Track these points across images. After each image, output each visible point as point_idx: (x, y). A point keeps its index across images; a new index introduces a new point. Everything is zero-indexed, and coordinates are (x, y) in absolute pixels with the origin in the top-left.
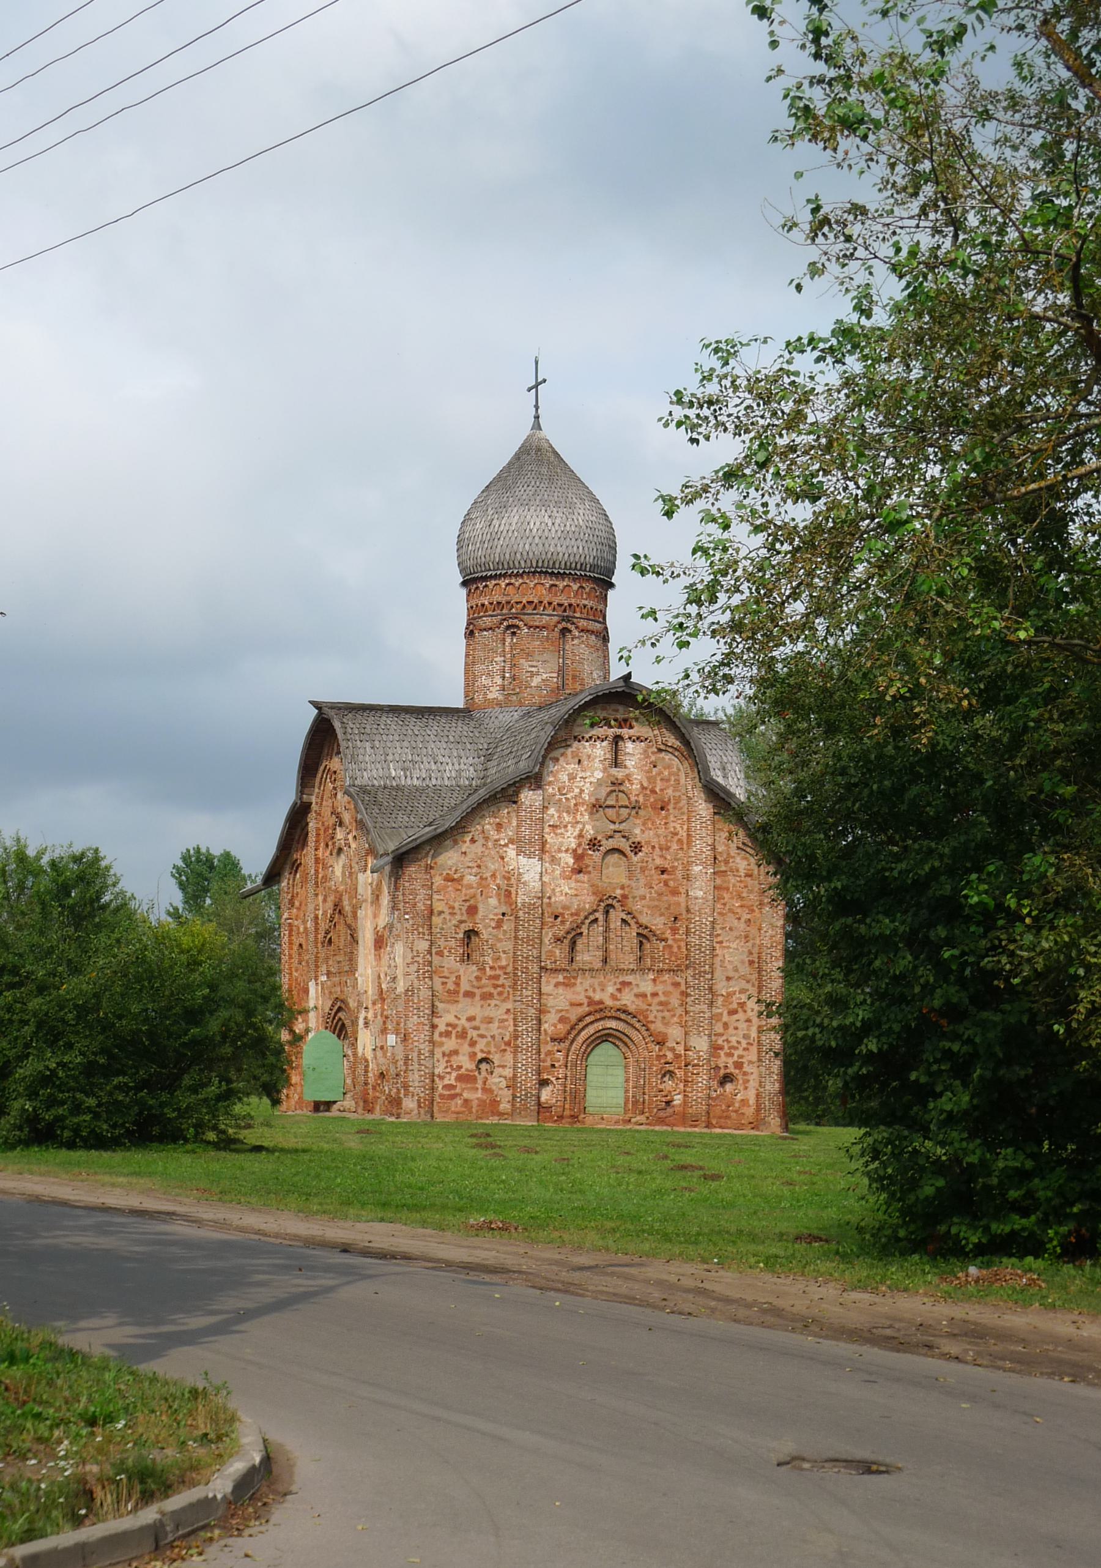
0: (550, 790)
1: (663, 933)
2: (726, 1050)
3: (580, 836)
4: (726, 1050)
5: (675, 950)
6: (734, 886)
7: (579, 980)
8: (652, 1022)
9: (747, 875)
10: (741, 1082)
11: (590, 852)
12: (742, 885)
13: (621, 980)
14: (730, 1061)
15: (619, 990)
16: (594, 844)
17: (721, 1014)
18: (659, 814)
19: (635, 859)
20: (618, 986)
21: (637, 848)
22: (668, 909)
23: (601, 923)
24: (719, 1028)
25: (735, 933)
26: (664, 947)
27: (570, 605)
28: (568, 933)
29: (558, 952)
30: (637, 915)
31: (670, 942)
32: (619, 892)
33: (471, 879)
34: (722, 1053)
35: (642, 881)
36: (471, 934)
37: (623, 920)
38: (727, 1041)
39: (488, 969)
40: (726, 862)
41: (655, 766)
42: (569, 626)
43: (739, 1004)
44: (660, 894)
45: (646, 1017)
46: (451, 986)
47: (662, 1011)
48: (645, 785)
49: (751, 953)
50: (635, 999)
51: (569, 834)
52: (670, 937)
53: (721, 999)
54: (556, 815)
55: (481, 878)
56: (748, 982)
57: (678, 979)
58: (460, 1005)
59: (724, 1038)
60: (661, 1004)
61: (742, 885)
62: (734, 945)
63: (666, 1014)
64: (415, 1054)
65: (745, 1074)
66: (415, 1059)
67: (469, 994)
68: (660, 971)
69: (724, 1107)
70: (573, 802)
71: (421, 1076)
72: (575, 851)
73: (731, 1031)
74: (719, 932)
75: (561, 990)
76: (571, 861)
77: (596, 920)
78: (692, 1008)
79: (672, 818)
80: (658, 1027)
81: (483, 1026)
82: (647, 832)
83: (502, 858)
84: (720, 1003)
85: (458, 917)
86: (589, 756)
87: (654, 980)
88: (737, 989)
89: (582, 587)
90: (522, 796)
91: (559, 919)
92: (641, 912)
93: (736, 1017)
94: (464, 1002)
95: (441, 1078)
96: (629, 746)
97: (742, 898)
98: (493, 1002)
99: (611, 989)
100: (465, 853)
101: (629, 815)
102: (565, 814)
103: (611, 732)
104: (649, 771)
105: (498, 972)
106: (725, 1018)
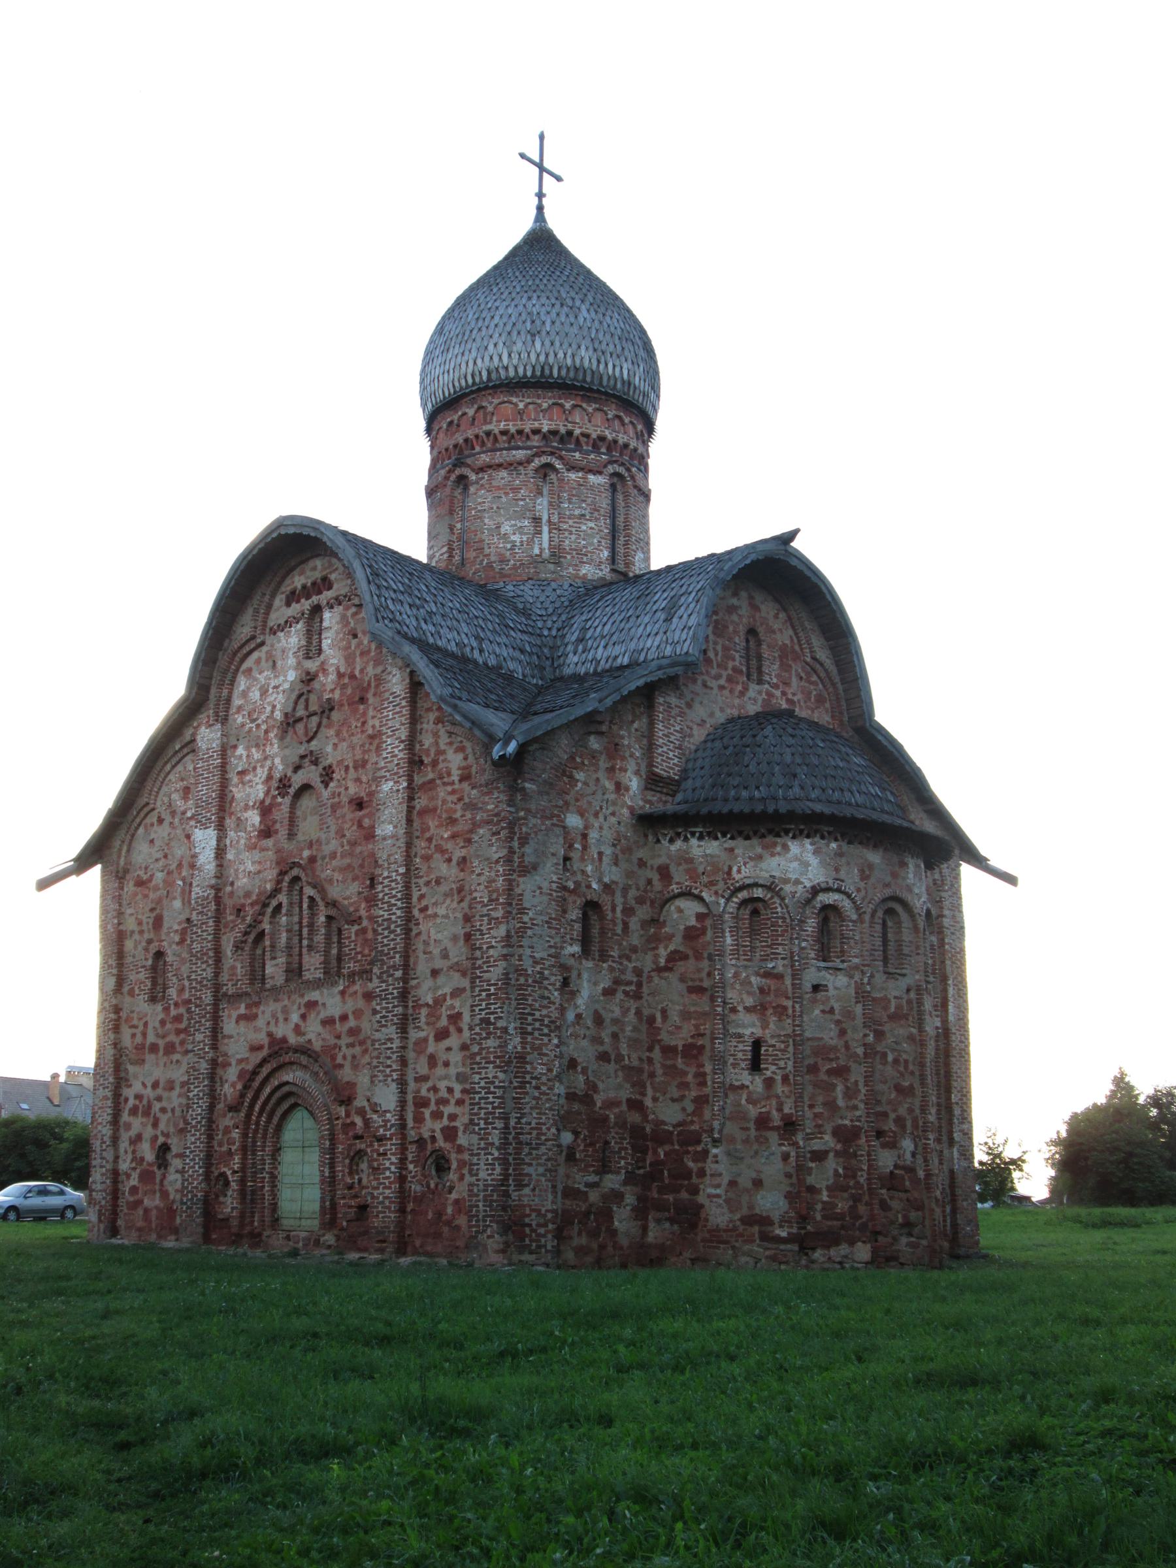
0: (240, 720)
1: (357, 910)
2: (433, 1107)
3: (270, 778)
4: (433, 1107)
5: (370, 935)
6: (444, 801)
7: (262, 1008)
8: (341, 1066)
9: (463, 779)
10: (454, 1165)
11: (279, 800)
12: (454, 798)
13: (306, 999)
14: (438, 1126)
15: (303, 1017)
16: (284, 784)
17: (425, 1040)
18: (357, 710)
19: (326, 794)
20: (303, 1011)
21: (327, 775)
22: (362, 866)
23: (284, 911)
24: (423, 1068)
25: (444, 888)
26: (357, 934)
27: (466, 440)
28: (246, 933)
29: (239, 966)
30: (327, 886)
31: (365, 923)
32: (306, 853)
33: (159, 876)
34: (427, 1113)
35: (333, 828)
36: (159, 955)
37: (311, 899)
38: (435, 1089)
39: (172, 1007)
40: (435, 763)
41: (355, 636)
42: (465, 471)
43: (450, 1017)
44: (353, 844)
45: (333, 1058)
46: (139, 1039)
47: (352, 1045)
48: (342, 670)
49: (467, 919)
50: (319, 1028)
51: (257, 780)
52: (363, 913)
53: (424, 1012)
54: (245, 753)
55: (168, 873)
56: (464, 974)
57: (370, 986)
58: (147, 1066)
59: (430, 1084)
60: (353, 1032)
61: (454, 798)
62: (441, 911)
63: (357, 1050)
64: (98, 1143)
65: (460, 1150)
66: (98, 1149)
67: (154, 1048)
68: (352, 975)
69: (430, 1215)
70: (264, 727)
71: (102, 1175)
72: (262, 802)
73: (440, 1071)
74: (424, 890)
75: (242, 1027)
76: (254, 818)
77: (279, 907)
78: (377, 1035)
79: (371, 713)
80: (346, 1074)
81: (165, 1095)
82: (339, 747)
83: (188, 837)
84: (423, 1019)
85: (146, 936)
86: (283, 651)
87: (343, 993)
88: (447, 990)
89: (481, 408)
90: (198, 738)
91: (242, 914)
92: (331, 881)
93: (447, 1043)
94: (150, 1058)
95: (128, 1176)
96: (327, 615)
97: (452, 821)
98: (176, 1057)
99: (295, 1018)
100: (152, 841)
101: (319, 725)
102: (254, 750)
103: (306, 605)
104: (348, 647)
105: (182, 1010)
106: (431, 1048)
